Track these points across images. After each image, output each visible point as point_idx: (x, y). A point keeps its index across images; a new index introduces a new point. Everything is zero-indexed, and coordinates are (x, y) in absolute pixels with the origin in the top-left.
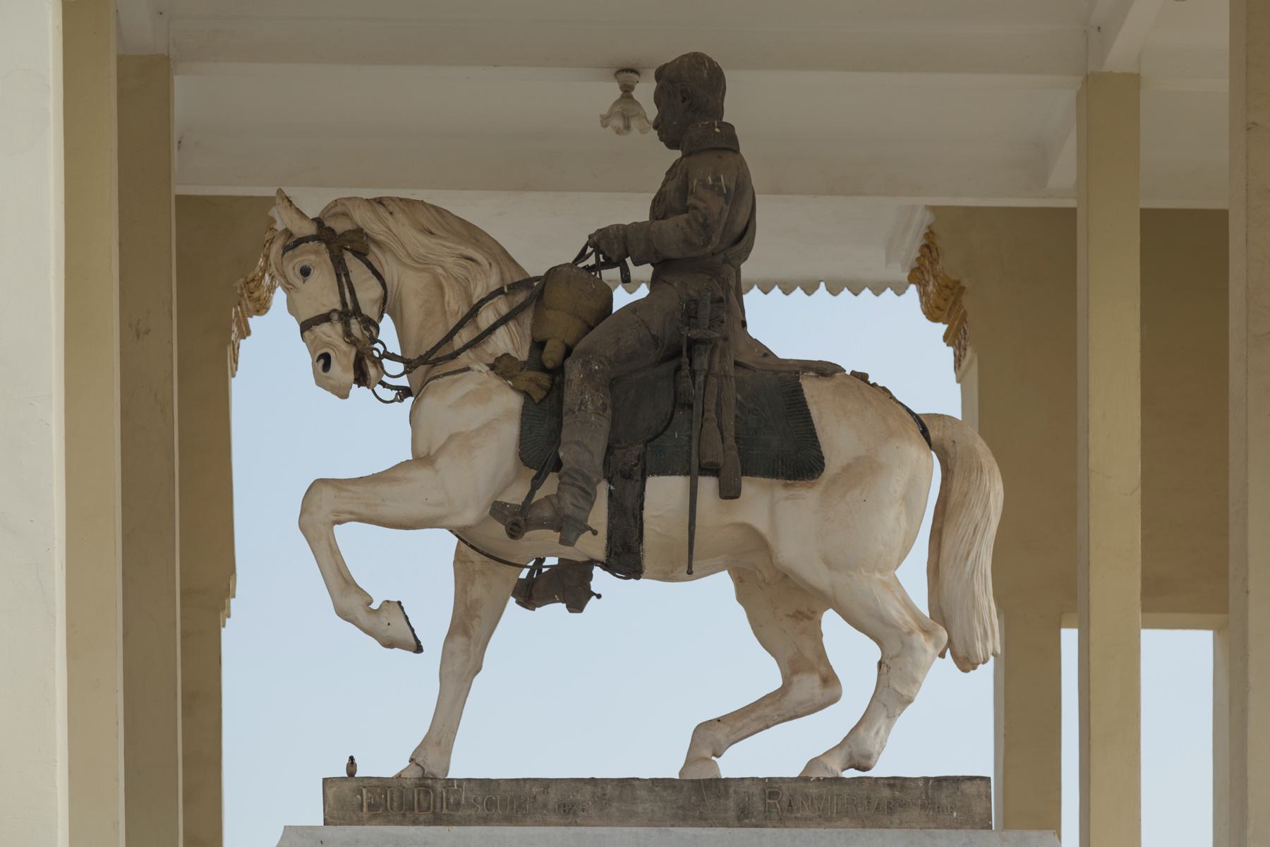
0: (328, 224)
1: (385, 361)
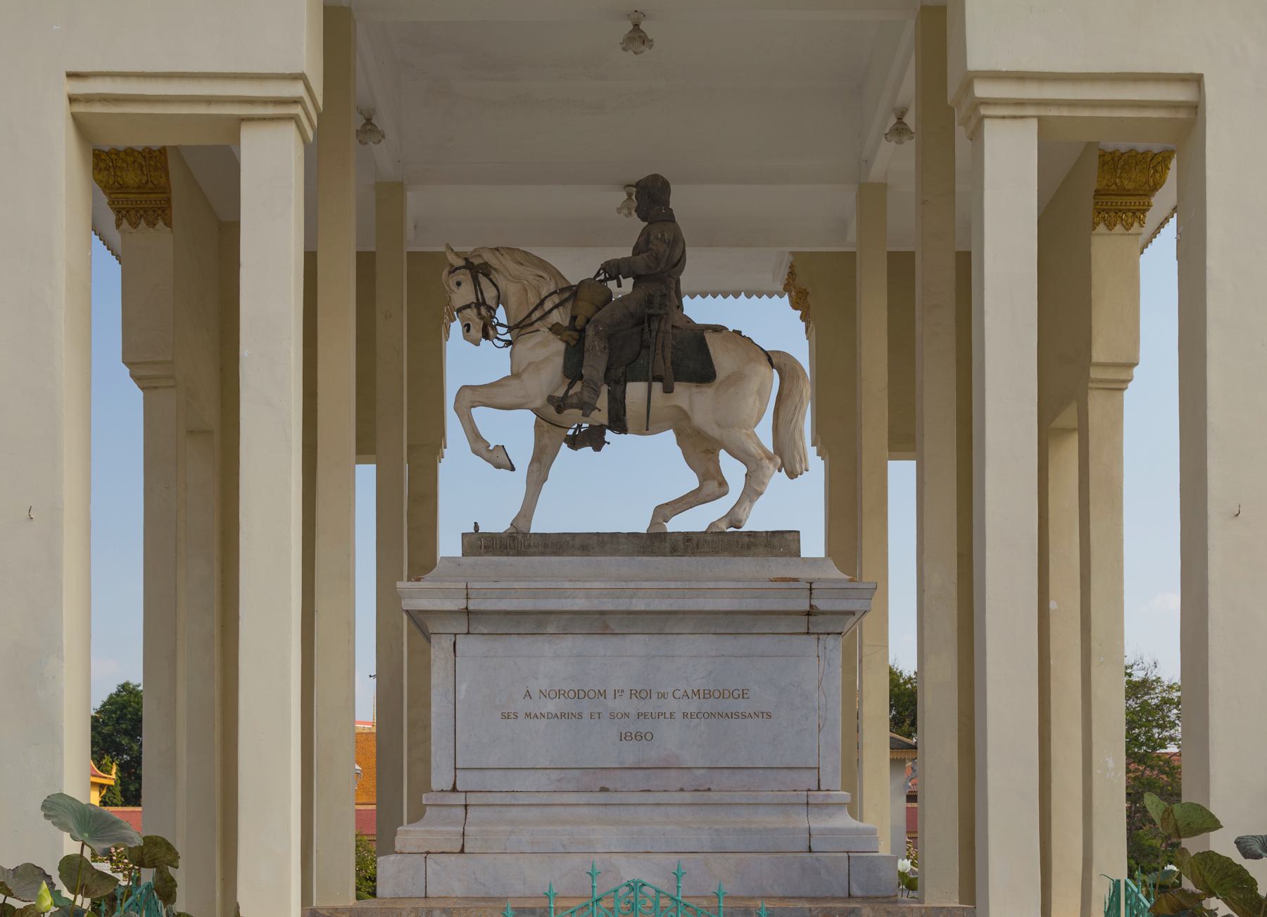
0: (470, 260)
1: (498, 327)
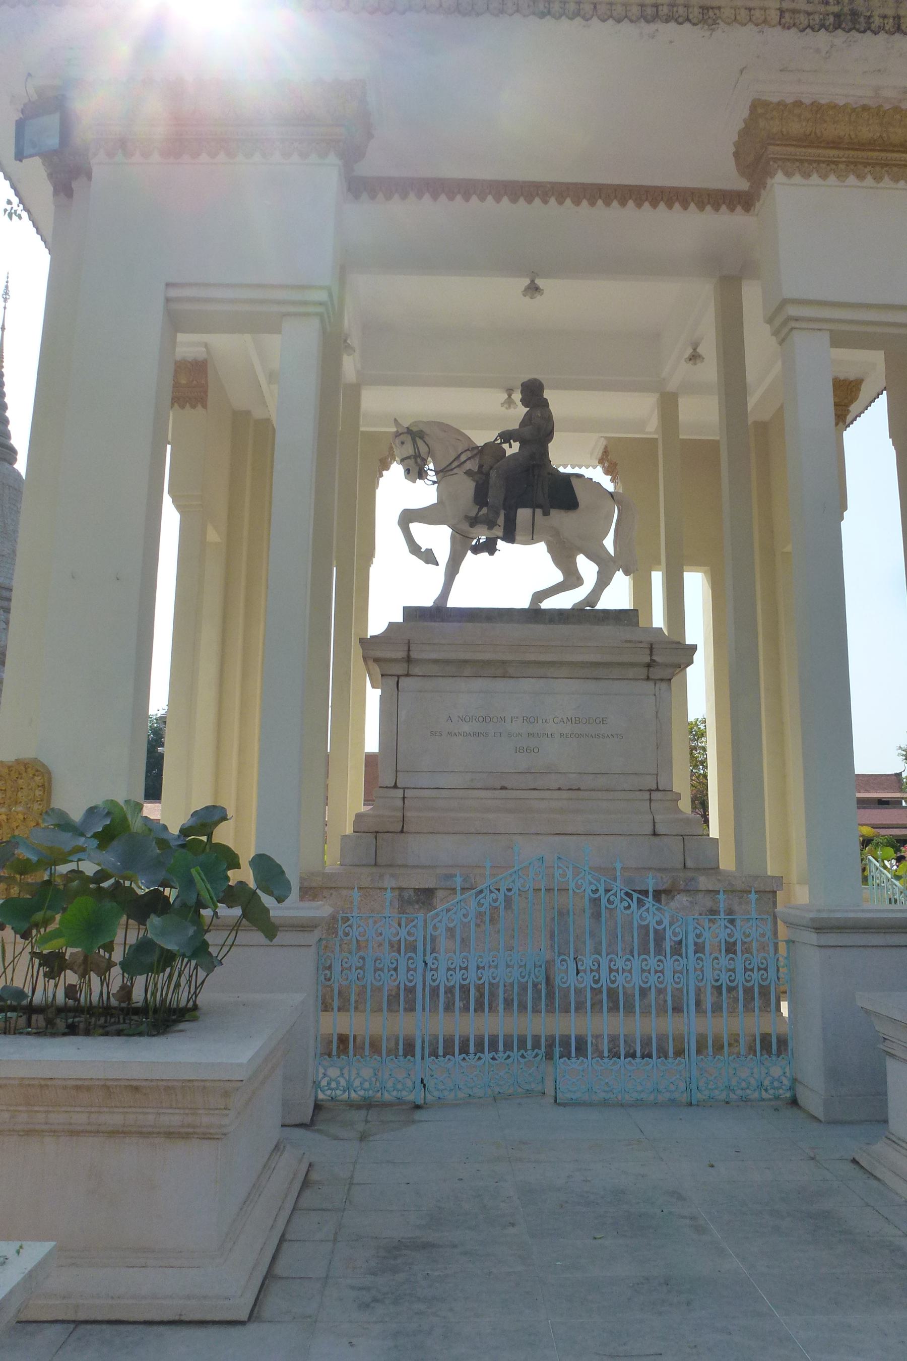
0: (410, 428)
1: (428, 471)
